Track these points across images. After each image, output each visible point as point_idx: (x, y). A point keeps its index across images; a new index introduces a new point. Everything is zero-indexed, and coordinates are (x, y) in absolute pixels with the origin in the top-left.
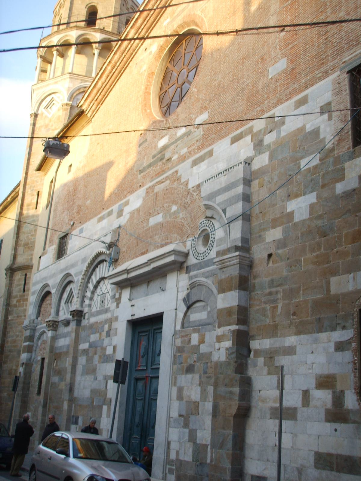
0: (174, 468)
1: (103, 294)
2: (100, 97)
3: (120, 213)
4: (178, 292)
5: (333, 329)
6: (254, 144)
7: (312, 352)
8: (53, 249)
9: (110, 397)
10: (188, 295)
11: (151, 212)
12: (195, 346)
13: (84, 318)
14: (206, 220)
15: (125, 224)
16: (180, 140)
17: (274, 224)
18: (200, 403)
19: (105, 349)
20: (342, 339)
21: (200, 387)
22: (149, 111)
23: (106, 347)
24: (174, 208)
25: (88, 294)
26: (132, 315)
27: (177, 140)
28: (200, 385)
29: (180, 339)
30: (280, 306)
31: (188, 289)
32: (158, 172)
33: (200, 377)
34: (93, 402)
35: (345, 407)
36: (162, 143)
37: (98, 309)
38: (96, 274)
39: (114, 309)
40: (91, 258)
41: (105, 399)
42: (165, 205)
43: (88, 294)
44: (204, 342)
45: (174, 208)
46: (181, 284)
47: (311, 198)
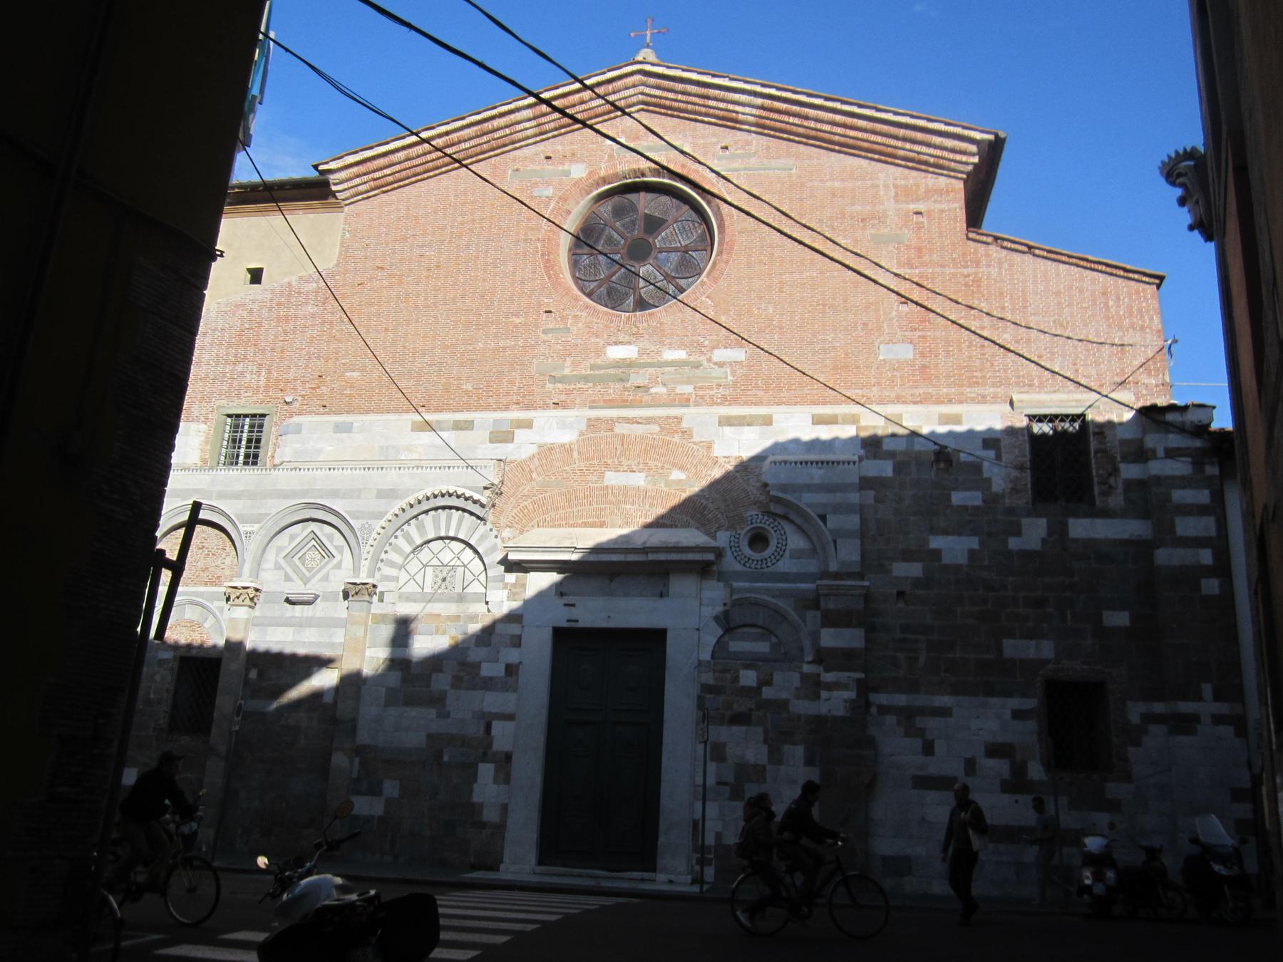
0: (712, 856)
1: (443, 565)
2: (390, 179)
3: (502, 436)
4: (701, 604)
5: (1008, 694)
7: (978, 717)
8: (200, 431)
9: (507, 748)
13: (381, 600)
14: (764, 516)
15: (525, 461)
16: (675, 368)
17: (908, 556)
18: (769, 768)
19: (477, 666)
20: (1022, 707)
21: (766, 746)
22: (561, 276)
23: (480, 662)
26: (568, 621)
27: (662, 365)
28: (765, 742)
29: (711, 674)
30: (922, 658)
31: (725, 604)
33: (766, 732)
34: (439, 755)
35: (1029, 778)
36: (617, 353)
39: (502, 602)
41: (485, 754)
42: (651, 463)
47: (973, 542)
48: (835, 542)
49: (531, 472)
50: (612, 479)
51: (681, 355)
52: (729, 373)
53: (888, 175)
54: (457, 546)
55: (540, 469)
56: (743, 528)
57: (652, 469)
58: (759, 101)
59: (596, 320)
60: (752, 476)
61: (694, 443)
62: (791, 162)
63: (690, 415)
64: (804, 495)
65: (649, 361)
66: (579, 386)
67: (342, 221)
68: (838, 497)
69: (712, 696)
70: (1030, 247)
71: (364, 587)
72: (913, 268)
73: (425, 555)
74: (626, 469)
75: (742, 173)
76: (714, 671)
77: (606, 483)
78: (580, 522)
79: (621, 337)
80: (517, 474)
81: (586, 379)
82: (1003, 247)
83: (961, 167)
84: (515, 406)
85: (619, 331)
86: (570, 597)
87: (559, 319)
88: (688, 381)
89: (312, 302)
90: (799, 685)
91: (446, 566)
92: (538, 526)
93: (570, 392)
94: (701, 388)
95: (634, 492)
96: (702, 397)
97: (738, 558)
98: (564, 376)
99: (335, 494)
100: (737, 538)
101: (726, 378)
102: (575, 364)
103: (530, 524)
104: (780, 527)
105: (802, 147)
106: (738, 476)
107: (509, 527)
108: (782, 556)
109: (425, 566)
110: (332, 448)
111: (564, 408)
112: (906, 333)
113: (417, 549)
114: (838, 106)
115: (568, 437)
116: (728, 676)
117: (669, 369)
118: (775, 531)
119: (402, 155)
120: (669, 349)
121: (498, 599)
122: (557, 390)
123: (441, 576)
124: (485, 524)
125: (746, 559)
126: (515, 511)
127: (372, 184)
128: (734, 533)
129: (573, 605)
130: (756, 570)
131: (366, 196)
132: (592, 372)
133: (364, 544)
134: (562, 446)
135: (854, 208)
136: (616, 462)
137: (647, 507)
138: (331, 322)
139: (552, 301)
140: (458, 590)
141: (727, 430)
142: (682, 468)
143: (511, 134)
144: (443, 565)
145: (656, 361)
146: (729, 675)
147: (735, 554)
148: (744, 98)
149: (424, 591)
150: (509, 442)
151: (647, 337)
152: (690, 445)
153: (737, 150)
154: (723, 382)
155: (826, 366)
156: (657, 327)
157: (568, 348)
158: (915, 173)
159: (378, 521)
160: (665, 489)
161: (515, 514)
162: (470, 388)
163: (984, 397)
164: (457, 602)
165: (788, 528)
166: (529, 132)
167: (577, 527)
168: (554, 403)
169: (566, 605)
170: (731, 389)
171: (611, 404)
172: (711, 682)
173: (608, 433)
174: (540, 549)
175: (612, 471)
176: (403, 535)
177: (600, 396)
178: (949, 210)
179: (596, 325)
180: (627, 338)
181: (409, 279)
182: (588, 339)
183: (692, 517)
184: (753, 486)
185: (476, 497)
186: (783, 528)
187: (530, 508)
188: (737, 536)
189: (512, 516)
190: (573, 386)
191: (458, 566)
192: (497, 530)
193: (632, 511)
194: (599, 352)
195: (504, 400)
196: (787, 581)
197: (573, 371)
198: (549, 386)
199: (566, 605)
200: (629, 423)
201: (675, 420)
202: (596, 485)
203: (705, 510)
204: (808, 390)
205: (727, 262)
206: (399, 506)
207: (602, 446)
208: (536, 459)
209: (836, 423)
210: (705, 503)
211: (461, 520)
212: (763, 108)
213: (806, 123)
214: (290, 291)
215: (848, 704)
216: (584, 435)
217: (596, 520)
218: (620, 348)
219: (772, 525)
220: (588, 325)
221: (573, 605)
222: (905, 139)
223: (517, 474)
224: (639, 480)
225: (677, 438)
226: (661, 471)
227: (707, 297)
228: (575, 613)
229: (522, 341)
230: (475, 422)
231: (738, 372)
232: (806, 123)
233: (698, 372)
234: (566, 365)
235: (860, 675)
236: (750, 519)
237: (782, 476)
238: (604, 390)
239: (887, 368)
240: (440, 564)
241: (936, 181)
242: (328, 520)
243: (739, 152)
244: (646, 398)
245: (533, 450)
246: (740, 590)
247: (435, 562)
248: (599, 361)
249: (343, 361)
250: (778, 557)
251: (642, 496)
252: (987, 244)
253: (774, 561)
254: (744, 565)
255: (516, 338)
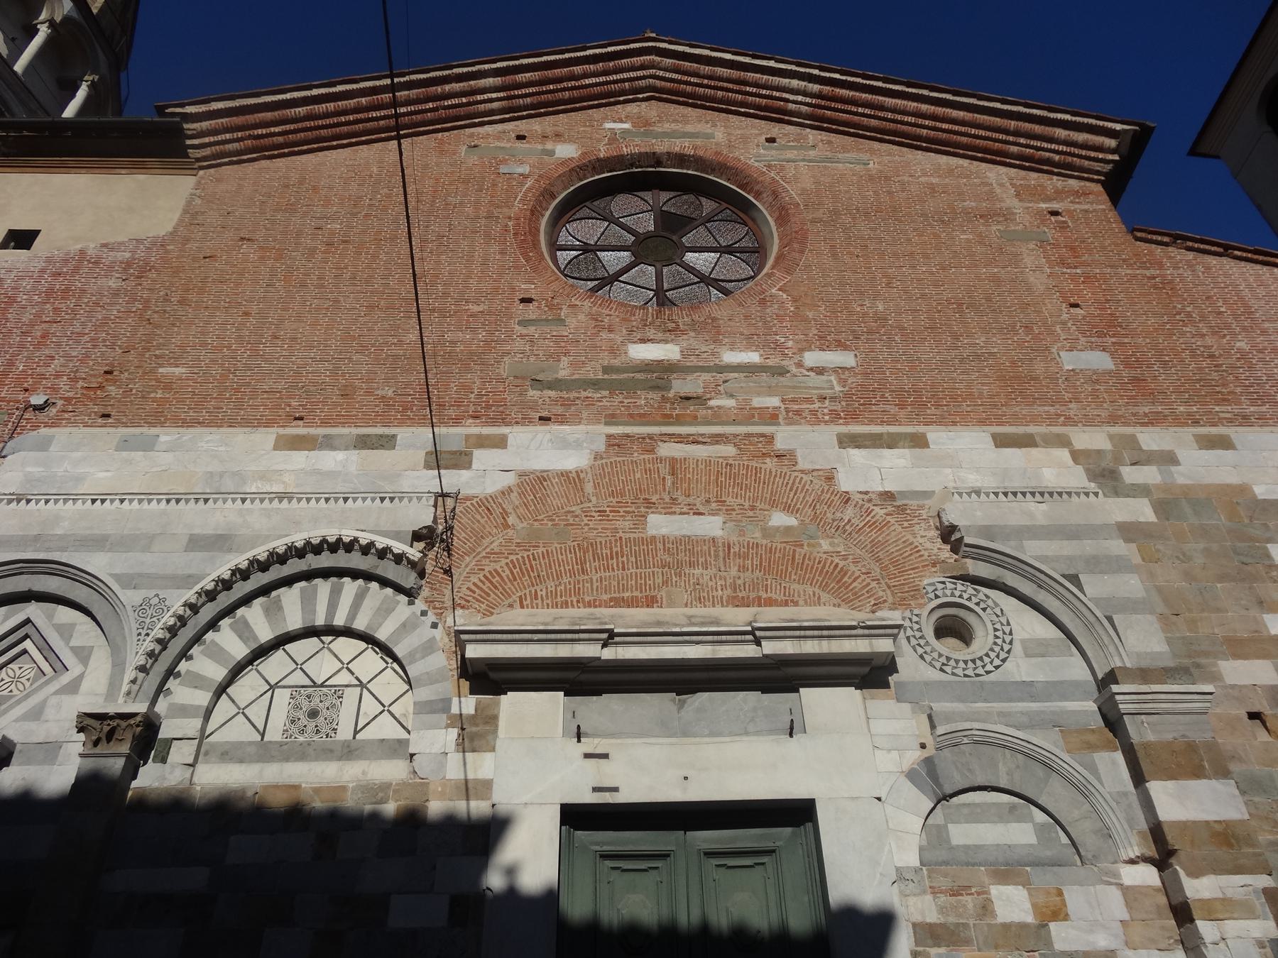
2: (281, 139)
6: (1087, 471)
10: (929, 763)
11: (654, 499)
12: (1023, 926)
14: (955, 584)
15: (493, 497)
16: (745, 374)
24: (780, 519)
25: (210, 669)
26: (595, 789)
29: (929, 897)
31: (923, 746)
32: (642, 411)
37: (274, 734)
38: (280, 608)
40: (280, 545)
43: (210, 669)
44: (1066, 917)
45: (780, 519)
46: (878, 726)
48: (1110, 619)
49: (505, 514)
50: (660, 524)
51: (753, 357)
52: (835, 382)
53: (996, 174)
54: (346, 646)
55: (521, 510)
56: (921, 606)
57: (734, 510)
58: (816, 88)
59: (607, 312)
60: (916, 520)
61: (802, 471)
62: (865, 157)
63: (785, 437)
64: (1027, 543)
65: (700, 364)
66: (584, 394)
67: (192, 185)
68: (1089, 547)
69: (942, 950)
70: (1226, 248)
71: (124, 724)
72: (1071, 268)
73: (275, 665)
74: (685, 510)
75: (802, 164)
76: (935, 891)
77: (651, 531)
78: (605, 597)
79: (651, 333)
80: (478, 517)
81: (595, 384)
82: (1189, 249)
83: (1097, 166)
84: (471, 421)
85: (646, 325)
86: (596, 741)
87: (547, 309)
88: (770, 391)
89: (117, 275)
90: (1126, 917)
91: (322, 685)
92: (522, 607)
93: (567, 403)
94: (793, 401)
95: (705, 548)
96: (798, 413)
97: (928, 658)
98: (558, 381)
99: (98, 543)
100: (917, 623)
101: (832, 388)
102: (574, 365)
103: (507, 602)
104: (990, 602)
105: (876, 145)
106: (893, 521)
107: (463, 607)
108: (1009, 652)
109: (272, 688)
110: (109, 474)
111: (562, 423)
112: (1093, 340)
113: (262, 652)
114: (925, 92)
115: (573, 461)
116: (969, 901)
117: (736, 375)
118: (984, 610)
119: (301, 111)
120: (731, 350)
121: (437, 749)
122: (547, 400)
123: (306, 706)
124: (411, 603)
125: (943, 660)
126: (474, 579)
127: (249, 142)
128: (908, 614)
129: (605, 756)
130: (966, 679)
131: (237, 158)
132: (606, 377)
133: (142, 638)
134: (564, 475)
135: (965, 204)
136: (667, 500)
137: (734, 571)
138: (148, 301)
139: (533, 286)
140: (345, 733)
141: (857, 455)
142: (788, 509)
143: (469, 104)
144: (315, 685)
145: (712, 364)
146: (969, 898)
147: (920, 651)
148: (795, 83)
149: (265, 739)
150: (465, 468)
151: (692, 334)
152: (796, 474)
153: (789, 142)
154: (828, 392)
155: (986, 376)
156: (707, 324)
157: (563, 344)
158: (1034, 175)
159: (184, 591)
160: (764, 542)
161: (475, 584)
162: (390, 393)
163: (1245, 417)
164: (340, 759)
165: (1008, 603)
166: (495, 105)
167: (600, 606)
168: (541, 418)
169: (587, 756)
170: (844, 403)
171: (643, 419)
172: (932, 917)
173: (646, 457)
174: (536, 637)
175: (661, 513)
176: (231, 625)
177: (622, 409)
178: (1095, 210)
179: (608, 318)
180: (660, 335)
181: (293, 254)
182: (597, 334)
183: (824, 587)
184: (922, 537)
185: (398, 547)
186: (997, 605)
187: (503, 575)
188: (915, 618)
189: (468, 588)
190: (574, 394)
191: (347, 686)
192: (436, 614)
193: (706, 578)
194: (613, 351)
195: (452, 412)
196: (1033, 698)
197: (574, 374)
198: (533, 394)
199: (587, 756)
200: (681, 442)
201: (761, 439)
202: (632, 536)
203: (845, 574)
204: (968, 406)
205: (802, 252)
206: (232, 565)
207: (638, 476)
208: (514, 496)
209: (1035, 445)
210: (841, 564)
211: (359, 598)
212: (819, 96)
213: (881, 114)
214: (81, 261)
215: (1268, 950)
216: (602, 458)
217: (637, 594)
218: (649, 346)
219: (975, 600)
220: (595, 318)
221: (605, 756)
222: (1017, 133)
223: (478, 517)
224: (711, 526)
225: (770, 464)
226: (751, 513)
227: (779, 290)
228: (609, 773)
229: (484, 334)
230: (399, 437)
231: (849, 382)
232: (881, 114)
233: (784, 380)
234: (561, 366)
235: (1264, 881)
236: (930, 589)
237: (979, 513)
238: (630, 401)
239: (1082, 380)
240: (308, 682)
241: (1064, 183)
242: (71, 596)
243: (792, 144)
244: (702, 413)
245: (510, 480)
246: (949, 718)
247: (298, 679)
248: (616, 362)
249: (157, 352)
250: (1003, 655)
251: (721, 554)
252: (1166, 244)
253: (997, 662)
254: (941, 670)
255: (474, 331)
